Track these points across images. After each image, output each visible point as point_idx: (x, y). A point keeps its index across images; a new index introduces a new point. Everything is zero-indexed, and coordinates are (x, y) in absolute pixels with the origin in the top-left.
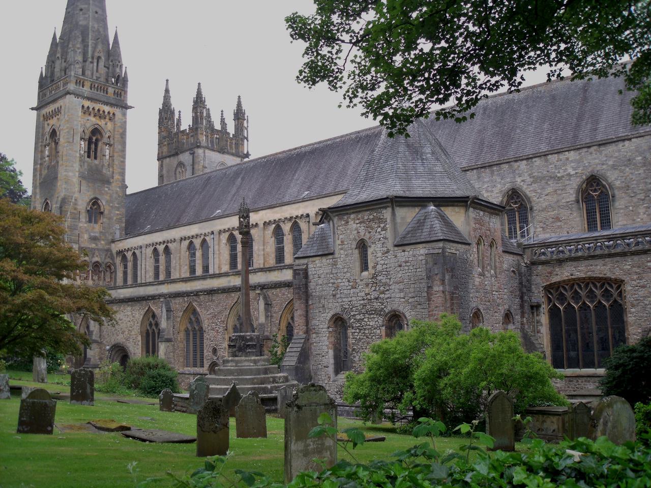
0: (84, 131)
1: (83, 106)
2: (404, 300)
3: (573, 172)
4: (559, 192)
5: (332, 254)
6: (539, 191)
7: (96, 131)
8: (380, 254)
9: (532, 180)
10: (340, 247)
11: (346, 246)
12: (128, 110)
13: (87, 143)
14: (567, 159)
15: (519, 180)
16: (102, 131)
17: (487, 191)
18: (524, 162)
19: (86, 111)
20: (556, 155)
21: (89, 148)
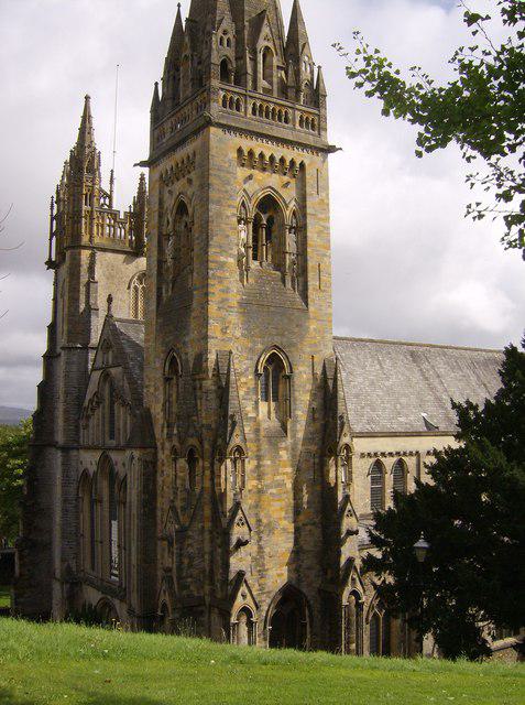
0: (243, 203)
1: (240, 151)
7: (269, 204)
12: (331, 156)
13: (251, 226)
16: (282, 204)
19: (247, 159)
21: (255, 239)
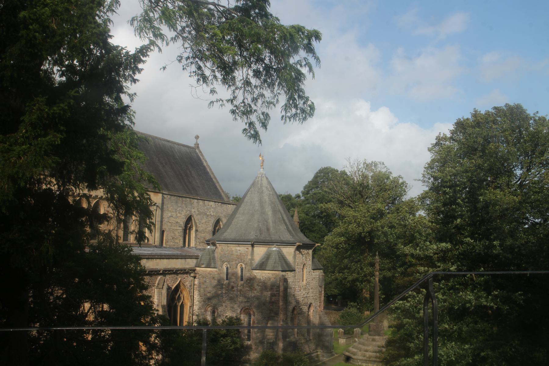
2: (312, 297)
3: (212, 214)
4: (207, 223)
5: (294, 271)
6: (200, 220)
8: (308, 273)
9: (198, 212)
10: (297, 266)
11: (299, 267)
14: (211, 206)
15: (193, 210)
17: (179, 213)
18: (196, 200)
20: (208, 202)
